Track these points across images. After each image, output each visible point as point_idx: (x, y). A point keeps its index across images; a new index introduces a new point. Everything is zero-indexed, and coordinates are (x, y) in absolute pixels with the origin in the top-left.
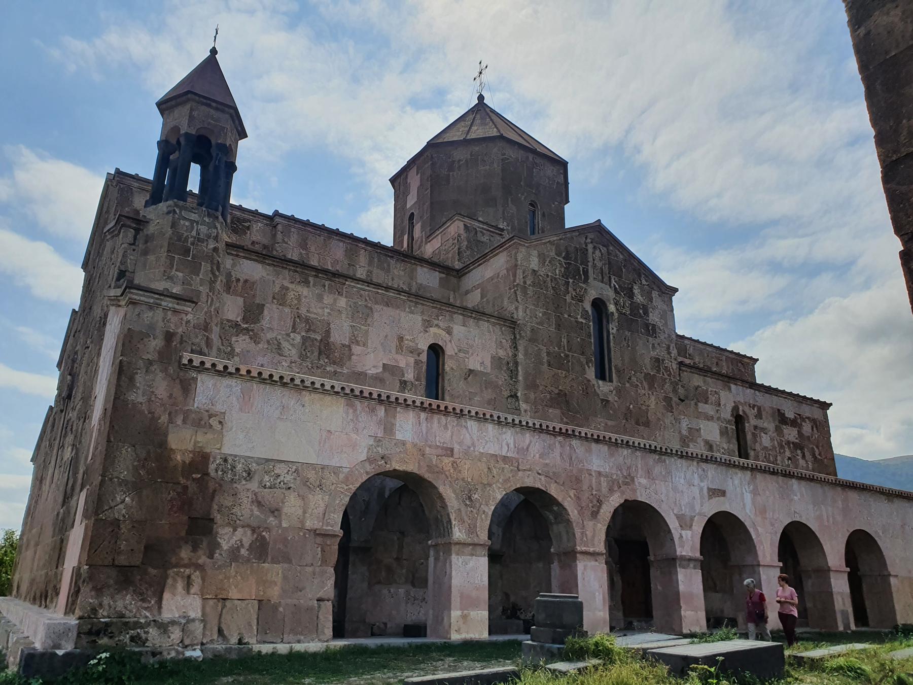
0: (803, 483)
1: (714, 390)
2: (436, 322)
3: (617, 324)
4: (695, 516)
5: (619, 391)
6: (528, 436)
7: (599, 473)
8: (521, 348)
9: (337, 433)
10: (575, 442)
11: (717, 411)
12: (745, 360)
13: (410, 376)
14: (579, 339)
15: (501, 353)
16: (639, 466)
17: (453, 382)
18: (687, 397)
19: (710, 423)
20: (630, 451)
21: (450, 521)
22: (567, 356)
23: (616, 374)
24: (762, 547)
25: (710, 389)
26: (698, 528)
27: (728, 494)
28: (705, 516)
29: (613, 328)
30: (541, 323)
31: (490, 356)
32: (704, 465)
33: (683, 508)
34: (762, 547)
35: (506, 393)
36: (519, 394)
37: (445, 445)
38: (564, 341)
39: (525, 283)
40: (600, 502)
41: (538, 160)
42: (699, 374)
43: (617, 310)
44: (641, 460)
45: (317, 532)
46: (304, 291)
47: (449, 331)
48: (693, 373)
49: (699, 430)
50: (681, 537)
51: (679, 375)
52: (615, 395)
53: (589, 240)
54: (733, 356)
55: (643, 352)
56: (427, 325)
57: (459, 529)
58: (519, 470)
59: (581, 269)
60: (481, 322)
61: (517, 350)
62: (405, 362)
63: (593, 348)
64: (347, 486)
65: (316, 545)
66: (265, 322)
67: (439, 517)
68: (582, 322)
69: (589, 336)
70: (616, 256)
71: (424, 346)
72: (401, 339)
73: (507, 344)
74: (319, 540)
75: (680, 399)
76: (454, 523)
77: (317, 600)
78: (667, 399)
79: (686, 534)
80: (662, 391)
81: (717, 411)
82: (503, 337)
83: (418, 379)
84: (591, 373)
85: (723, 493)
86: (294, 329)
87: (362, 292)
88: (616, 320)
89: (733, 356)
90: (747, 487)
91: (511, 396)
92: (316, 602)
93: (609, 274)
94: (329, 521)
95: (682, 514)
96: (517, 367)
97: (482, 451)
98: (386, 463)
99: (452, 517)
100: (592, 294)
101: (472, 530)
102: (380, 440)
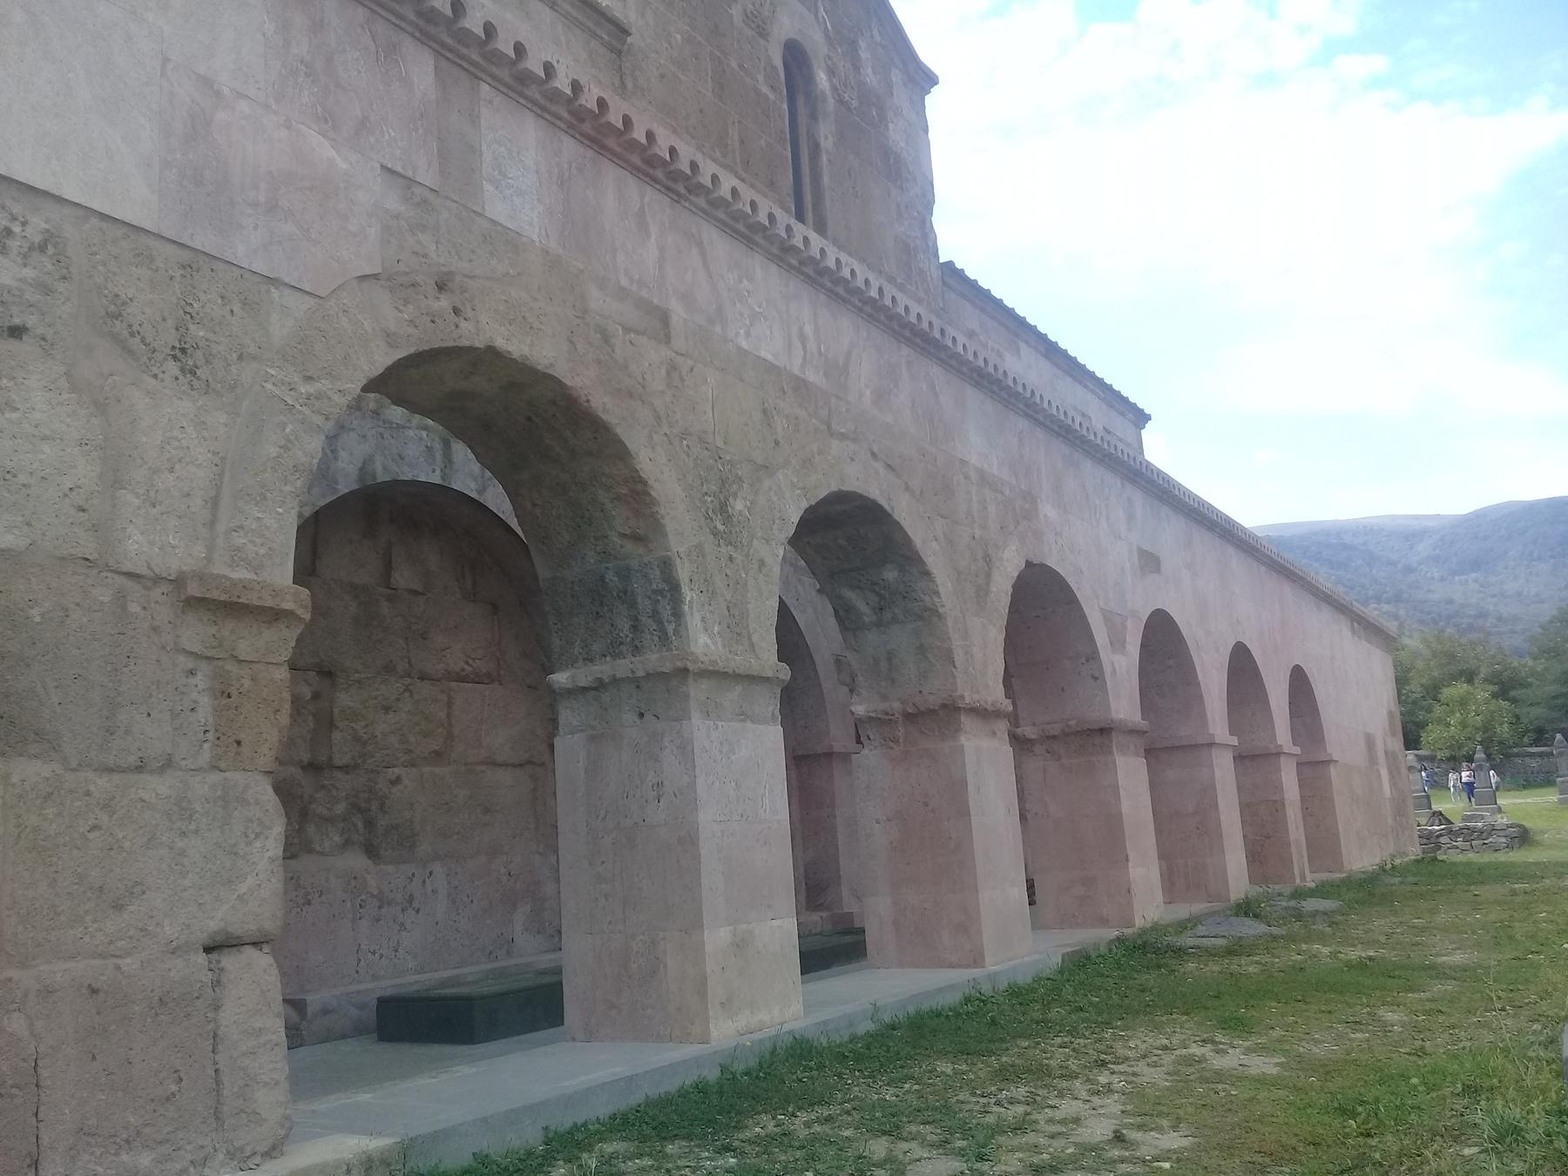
9: (243, 106)
14: (763, 143)
21: (675, 587)
37: (644, 293)
43: (834, 88)
45: (193, 589)
57: (703, 619)
58: (832, 435)
64: (308, 379)
65: (184, 662)
67: (611, 577)
74: (195, 633)
76: (688, 594)
77: (208, 950)
92: (202, 958)
94: (239, 540)
97: (745, 345)
98: (456, 311)
99: (683, 572)
101: (736, 629)
102: (425, 201)
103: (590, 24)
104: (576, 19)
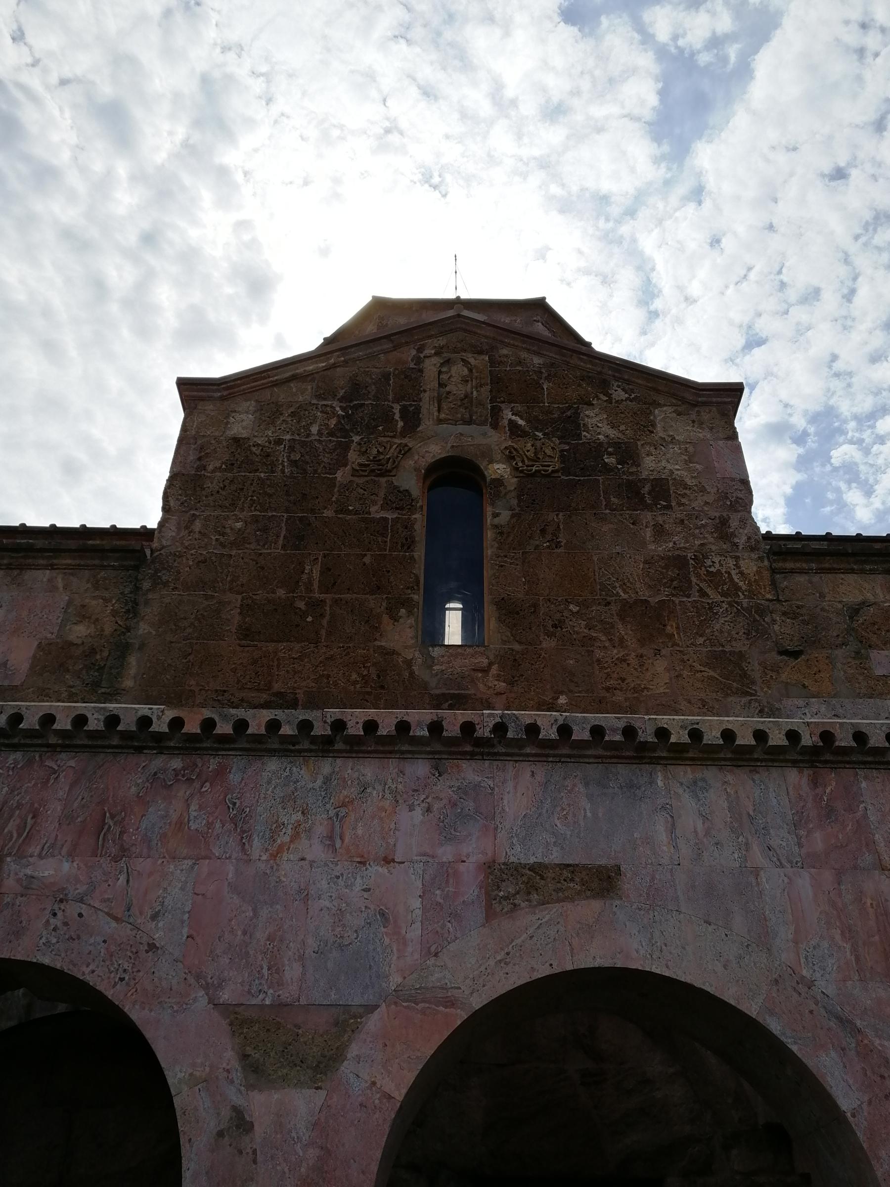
3: (515, 502)
4: (371, 1009)
15: (80, 631)
16: (55, 808)
20: (18, 755)
22: (315, 606)
28: (451, 1003)
31: (36, 643)
33: (292, 972)
42: (862, 572)
44: (72, 786)
51: (774, 583)
52: (498, 677)
53: (428, 351)
55: (618, 549)
60: (28, 575)
61: (136, 614)
68: (386, 519)
75: (784, 652)
80: (701, 640)
82: (97, 593)
90: (782, 838)
95: (280, 1006)
100: (435, 451)
103: (97, 562)
104: (79, 565)
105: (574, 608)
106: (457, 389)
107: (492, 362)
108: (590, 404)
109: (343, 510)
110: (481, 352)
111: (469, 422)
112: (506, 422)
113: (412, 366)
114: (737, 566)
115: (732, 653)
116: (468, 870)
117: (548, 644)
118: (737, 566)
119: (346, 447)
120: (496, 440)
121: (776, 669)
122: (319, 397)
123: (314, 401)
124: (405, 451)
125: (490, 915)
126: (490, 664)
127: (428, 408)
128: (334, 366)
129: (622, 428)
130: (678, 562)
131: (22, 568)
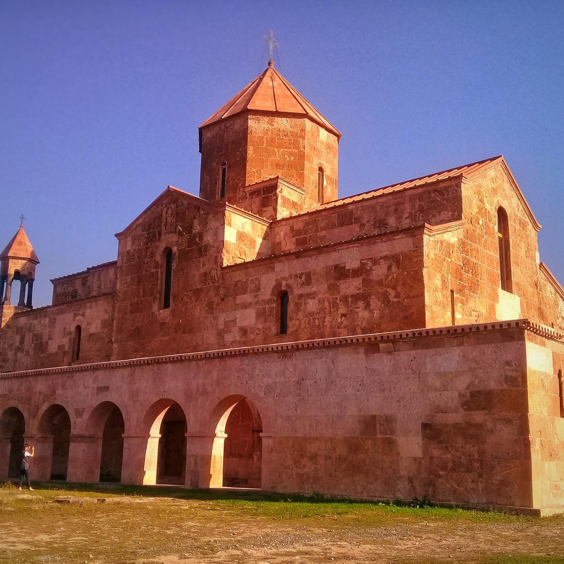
0: (178, 365)
1: (255, 277)
2: (79, 312)
5: (173, 311)
6: (14, 381)
7: (40, 393)
8: (117, 309)
10: (31, 379)
11: (256, 296)
12: (441, 185)
13: (66, 348)
14: (150, 286)
17: (85, 345)
18: (226, 295)
19: (246, 311)
22: (142, 301)
23: (172, 300)
24: (128, 423)
25: (250, 278)
26: (86, 416)
27: (110, 388)
28: (92, 407)
29: (174, 266)
30: (129, 286)
32: (97, 373)
34: (128, 423)
35: (106, 341)
36: (113, 339)
38: (141, 291)
39: (122, 263)
40: (38, 409)
41: (228, 124)
46: (36, 322)
47: (83, 315)
48: (234, 271)
49: (234, 321)
50: (75, 422)
53: (164, 206)
54: (420, 190)
55: (195, 272)
56: (75, 315)
59: (157, 232)
62: (65, 341)
63: (158, 288)
66: (25, 343)
69: (157, 280)
70: (182, 205)
71: (73, 329)
72: (65, 329)
73: (110, 309)
78: (210, 304)
79: (79, 420)
81: (256, 296)
83: (69, 348)
84: (155, 307)
85: (107, 388)
86: (32, 343)
87: (53, 312)
88: (177, 258)
89: (420, 190)
91: (109, 342)
93: (176, 223)
96: (113, 322)
100: (162, 246)
105: (185, 293)
106: (169, 219)
107: (177, 206)
108: (196, 218)
109: (147, 271)
110: (174, 203)
111: (171, 232)
112: (177, 230)
113: (161, 213)
114: (217, 273)
115: (211, 301)
116: (96, 389)
117: (180, 305)
118: (217, 273)
119: (147, 248)
120: (174, 238)
121: (218, 304)
122: (142, 231)
123: (142, 233)
124: (157, 247)
125: (97, 395)
126: (170, 313)
127: (163, 230)
128: (145, 219)
129: (201, 226)
130: (205, 274)
131: (97, 301)
